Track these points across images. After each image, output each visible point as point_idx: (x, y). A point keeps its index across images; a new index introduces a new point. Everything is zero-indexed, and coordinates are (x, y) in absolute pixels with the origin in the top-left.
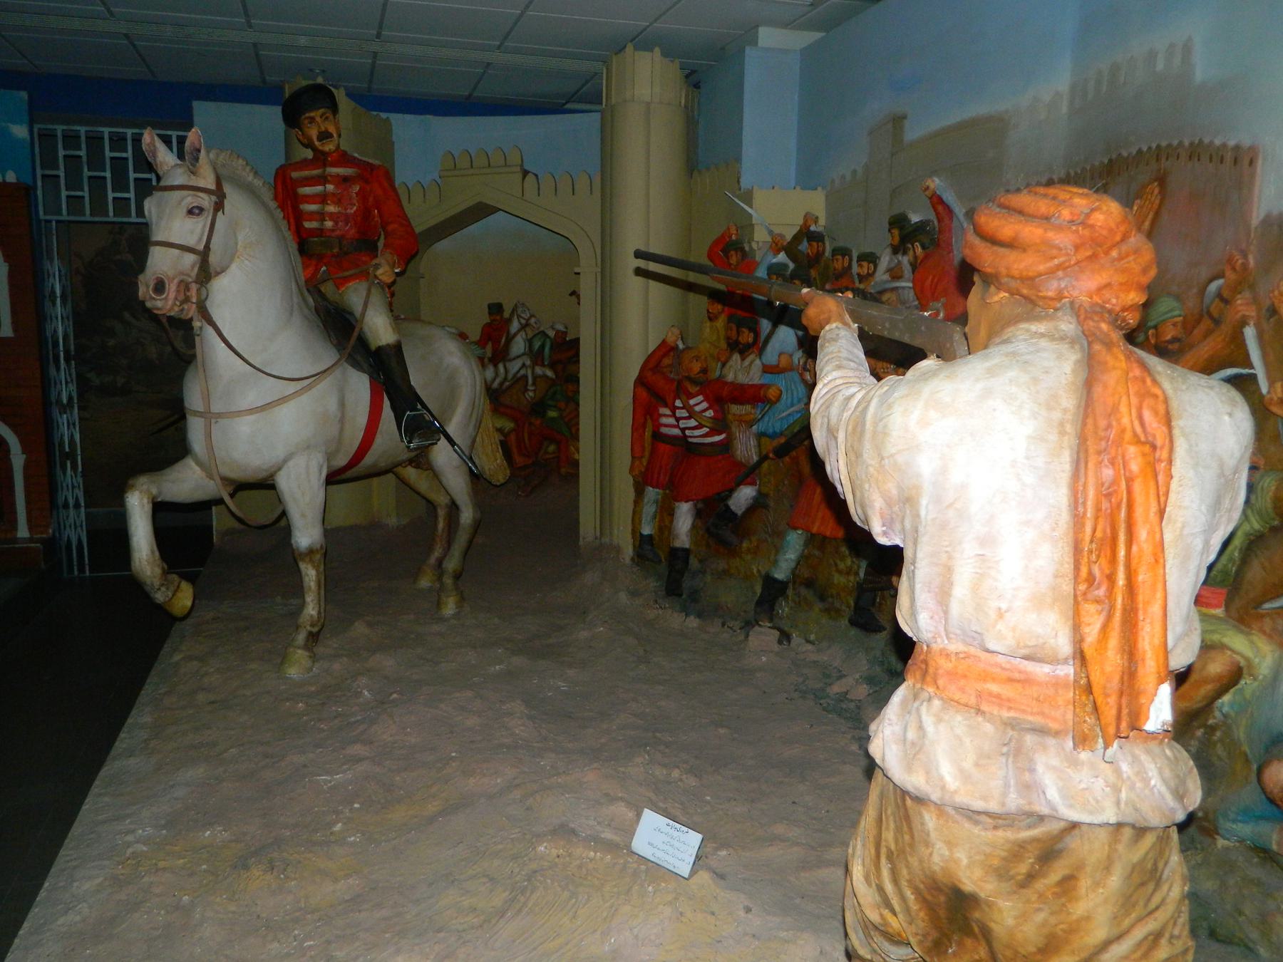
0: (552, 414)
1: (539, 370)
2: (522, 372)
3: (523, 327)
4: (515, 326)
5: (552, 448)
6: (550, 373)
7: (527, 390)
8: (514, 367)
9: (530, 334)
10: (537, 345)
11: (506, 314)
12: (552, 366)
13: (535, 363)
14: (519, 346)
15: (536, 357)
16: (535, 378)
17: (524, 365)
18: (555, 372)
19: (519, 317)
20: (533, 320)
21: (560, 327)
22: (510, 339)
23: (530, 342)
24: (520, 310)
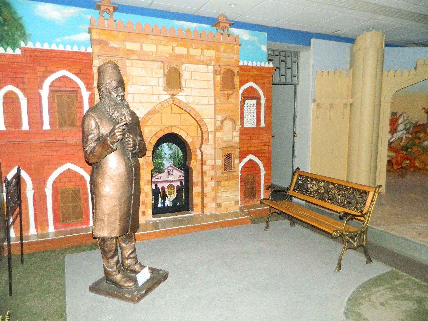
0: (409, 150)
1: (407, 135)
2: (402, 136)
3: (404, 121)
4: (401, 121)
5: (408, 162)
6: (410, 136)
7: (401, 142)
8: (399, 134)
9: (406, 122)
10: (408, 126)
11: (398, 117)
12: (411, 134)
13: (407, 133)
14: (401, 127)
15: (407, 130)
16: (406, 138)
17: (403, 134)
18: (412, 136)
19: (404, 116)
20: (409, 118)
21: (416, 120)
22: (398, 126)
23: (405, 125)
24: (405, 115)
